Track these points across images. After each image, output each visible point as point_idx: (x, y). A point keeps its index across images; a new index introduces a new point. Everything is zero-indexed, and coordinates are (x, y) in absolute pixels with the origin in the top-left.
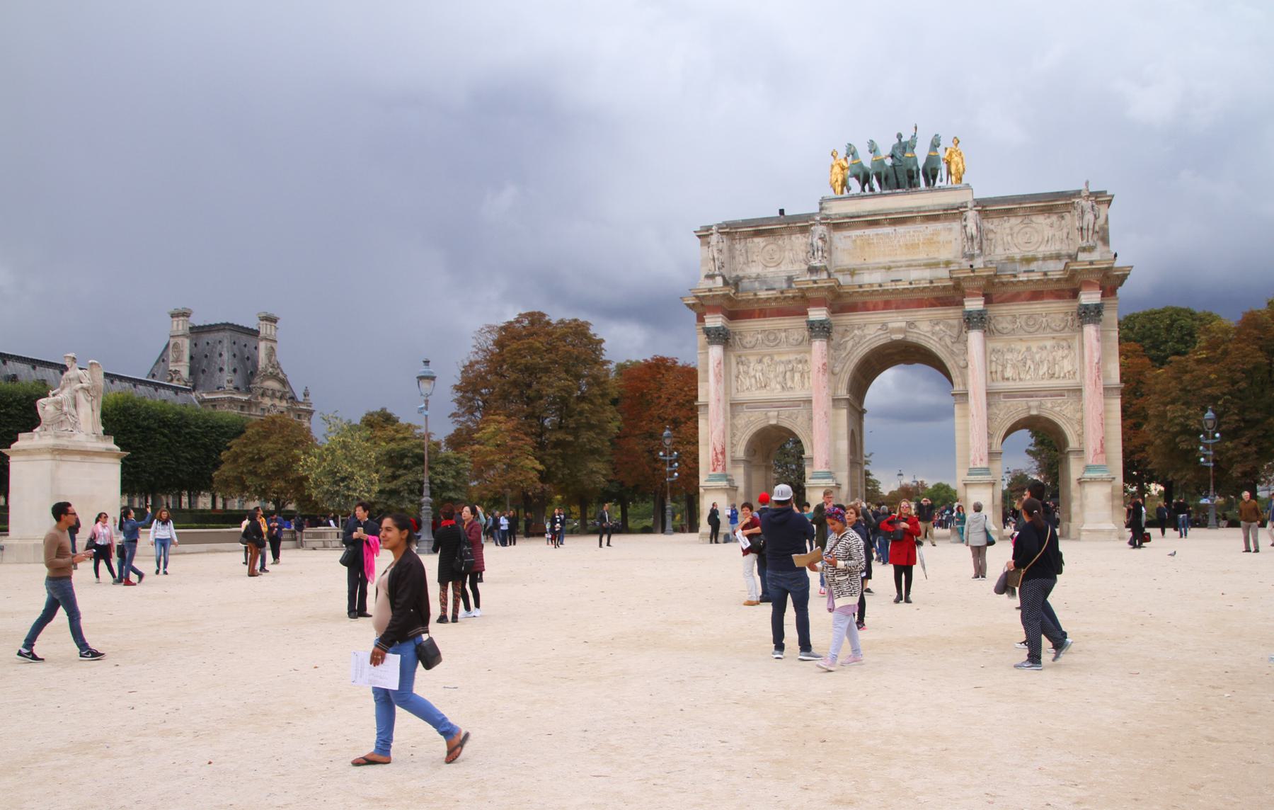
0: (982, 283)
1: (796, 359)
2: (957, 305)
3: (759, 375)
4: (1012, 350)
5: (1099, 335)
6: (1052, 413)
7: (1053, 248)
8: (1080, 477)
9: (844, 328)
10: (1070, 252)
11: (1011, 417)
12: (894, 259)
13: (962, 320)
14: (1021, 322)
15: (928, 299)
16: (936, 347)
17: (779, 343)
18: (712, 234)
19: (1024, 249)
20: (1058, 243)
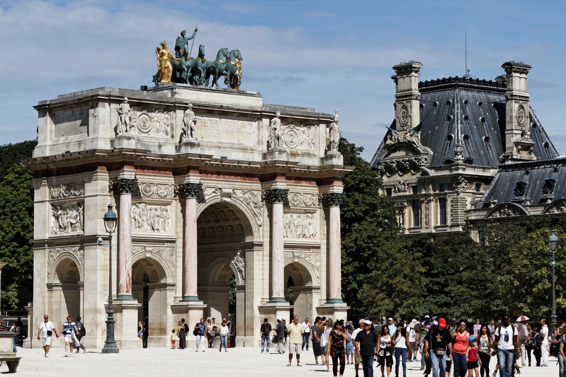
12: (219, 141)
19: (290, 146)
20: (307, 145)
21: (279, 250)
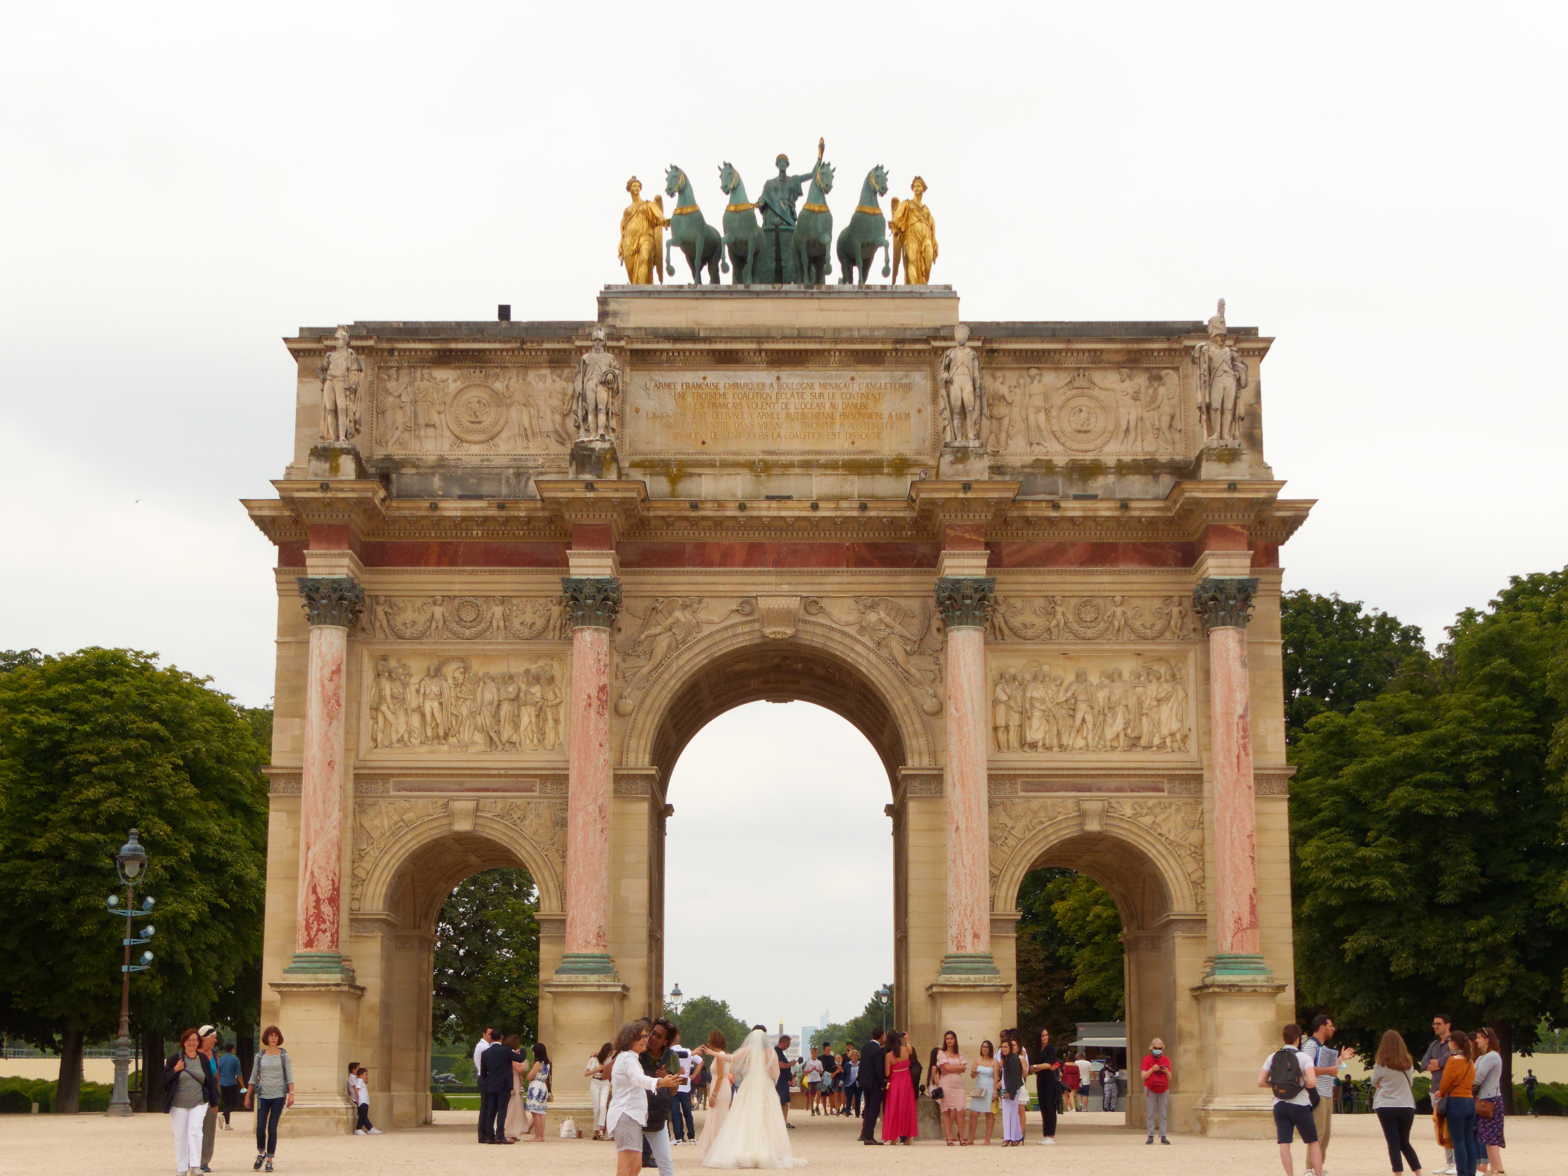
0: (984, 517)
1: (527, 672)
2: (919, 565)
3: (431, 706)
4: (1044, 677)
5: (1245, 653)
6: (1135, 830)
7: (1139, 449)
8: (1197, 983)
9: (648, 602)
10: (1177, 458)
11: (1041, 836)
13: (932, 602)
14: (1064, 612)
15: (852, 544)
16: (867, 659)
17: (485, 631)
18: (333, 348)
19: (1075, 446)
20: (1149, 438)
21: (958, 790)
